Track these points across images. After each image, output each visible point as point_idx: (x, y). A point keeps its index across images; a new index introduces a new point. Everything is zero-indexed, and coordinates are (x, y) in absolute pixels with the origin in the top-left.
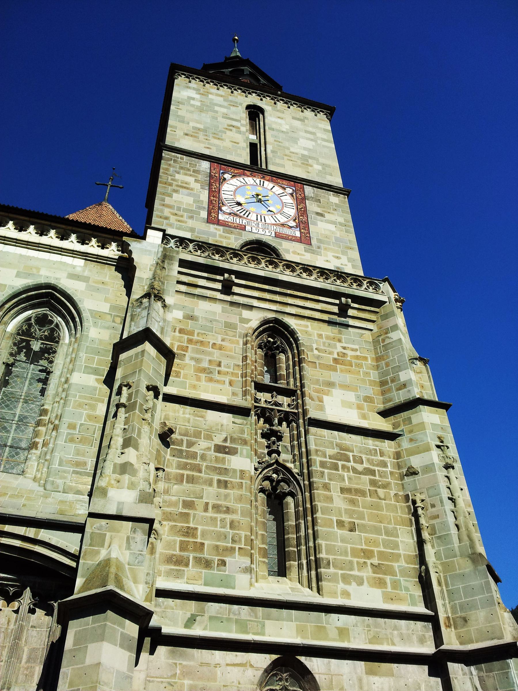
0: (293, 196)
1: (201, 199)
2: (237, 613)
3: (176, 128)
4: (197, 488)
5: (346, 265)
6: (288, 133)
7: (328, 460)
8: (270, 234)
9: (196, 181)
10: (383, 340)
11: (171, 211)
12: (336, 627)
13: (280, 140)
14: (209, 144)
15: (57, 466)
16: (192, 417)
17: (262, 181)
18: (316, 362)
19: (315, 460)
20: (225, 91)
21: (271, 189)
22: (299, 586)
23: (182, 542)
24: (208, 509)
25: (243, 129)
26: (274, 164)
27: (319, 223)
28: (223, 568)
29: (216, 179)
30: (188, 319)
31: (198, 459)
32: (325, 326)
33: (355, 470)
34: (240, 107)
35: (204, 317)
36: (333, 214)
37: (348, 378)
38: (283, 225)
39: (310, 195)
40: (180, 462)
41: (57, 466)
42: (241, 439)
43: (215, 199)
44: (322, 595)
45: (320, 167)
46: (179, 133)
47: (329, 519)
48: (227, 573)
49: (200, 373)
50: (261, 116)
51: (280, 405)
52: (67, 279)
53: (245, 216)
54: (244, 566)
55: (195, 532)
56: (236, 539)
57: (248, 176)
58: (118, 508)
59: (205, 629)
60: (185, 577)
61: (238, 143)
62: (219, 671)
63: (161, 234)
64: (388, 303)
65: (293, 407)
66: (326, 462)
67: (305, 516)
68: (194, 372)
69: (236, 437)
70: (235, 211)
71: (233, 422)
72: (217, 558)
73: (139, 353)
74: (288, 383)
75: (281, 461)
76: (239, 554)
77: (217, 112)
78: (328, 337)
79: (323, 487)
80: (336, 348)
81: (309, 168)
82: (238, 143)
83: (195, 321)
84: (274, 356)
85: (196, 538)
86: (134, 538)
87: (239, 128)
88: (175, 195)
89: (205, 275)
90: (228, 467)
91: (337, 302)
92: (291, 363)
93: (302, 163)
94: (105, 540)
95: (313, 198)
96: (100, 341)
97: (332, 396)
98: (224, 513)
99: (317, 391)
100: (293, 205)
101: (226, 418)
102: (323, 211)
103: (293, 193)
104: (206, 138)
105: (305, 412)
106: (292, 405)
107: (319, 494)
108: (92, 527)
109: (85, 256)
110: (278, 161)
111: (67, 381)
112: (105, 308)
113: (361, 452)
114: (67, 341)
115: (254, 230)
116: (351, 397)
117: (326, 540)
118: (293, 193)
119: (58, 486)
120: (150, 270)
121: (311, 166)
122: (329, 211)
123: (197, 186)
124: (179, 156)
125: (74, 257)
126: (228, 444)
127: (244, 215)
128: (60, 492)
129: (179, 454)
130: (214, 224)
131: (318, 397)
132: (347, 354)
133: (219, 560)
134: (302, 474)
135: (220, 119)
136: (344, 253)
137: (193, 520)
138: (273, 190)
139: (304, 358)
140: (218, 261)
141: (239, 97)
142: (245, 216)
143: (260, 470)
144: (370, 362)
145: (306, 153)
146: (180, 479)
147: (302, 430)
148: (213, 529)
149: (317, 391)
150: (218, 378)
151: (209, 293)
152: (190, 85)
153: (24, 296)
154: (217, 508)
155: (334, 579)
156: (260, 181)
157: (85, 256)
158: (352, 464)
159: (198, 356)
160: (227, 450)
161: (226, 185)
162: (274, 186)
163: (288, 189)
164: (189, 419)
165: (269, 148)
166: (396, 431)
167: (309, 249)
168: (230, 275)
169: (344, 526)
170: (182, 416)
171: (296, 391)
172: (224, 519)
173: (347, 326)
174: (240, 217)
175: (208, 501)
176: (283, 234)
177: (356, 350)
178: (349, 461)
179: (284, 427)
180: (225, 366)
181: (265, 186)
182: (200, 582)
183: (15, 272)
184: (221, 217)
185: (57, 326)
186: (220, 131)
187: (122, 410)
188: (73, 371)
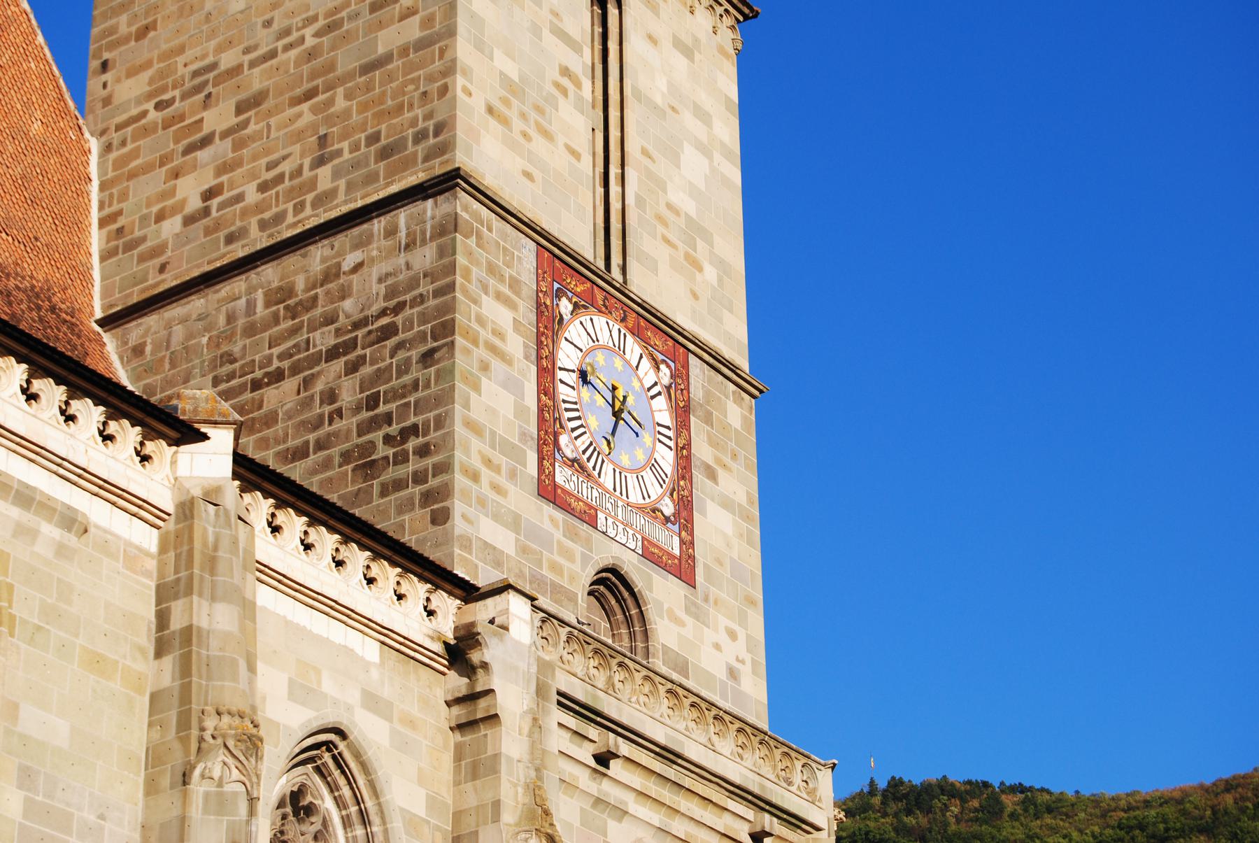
5: (743, 662)
64: (824, 834)
102: (718, 460)
109: (384, 633)
115: (612, 533)
145: (689, 206)
163: (663, 367)
184: (563, 476)
185: (325, 823)
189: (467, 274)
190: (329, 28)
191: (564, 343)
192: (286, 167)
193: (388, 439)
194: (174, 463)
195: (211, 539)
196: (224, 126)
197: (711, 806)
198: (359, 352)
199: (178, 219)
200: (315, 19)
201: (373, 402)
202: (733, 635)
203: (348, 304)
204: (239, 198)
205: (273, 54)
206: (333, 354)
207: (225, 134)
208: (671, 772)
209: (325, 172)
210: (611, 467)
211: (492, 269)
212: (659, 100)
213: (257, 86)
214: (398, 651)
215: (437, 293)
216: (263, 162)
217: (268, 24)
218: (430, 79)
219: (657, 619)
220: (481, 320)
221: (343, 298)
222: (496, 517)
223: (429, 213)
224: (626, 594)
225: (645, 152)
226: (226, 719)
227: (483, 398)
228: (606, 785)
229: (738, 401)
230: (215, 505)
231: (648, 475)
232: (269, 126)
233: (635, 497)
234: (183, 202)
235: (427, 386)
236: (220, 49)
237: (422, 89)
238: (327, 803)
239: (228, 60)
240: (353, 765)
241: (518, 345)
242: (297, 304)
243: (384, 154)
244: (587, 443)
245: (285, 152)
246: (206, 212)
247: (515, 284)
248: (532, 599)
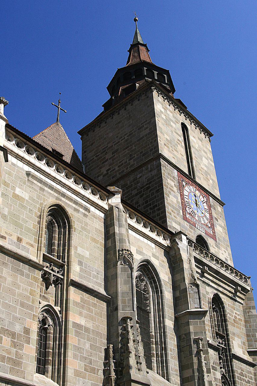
10: (248, 313)
14: (174, 154)
38: (207, 225)
70: (191, 211)
77: (172, 126)
114: (151, 294)
124: (166, 163)
134: (230, 381)
145: (205, 169)
163: (204, 198)
166: (253, 362)
173: (236, 301)
184: (188, 216)
185: (146, 283)
189: (164, 174)
190: (130, 135)
191: (185, 190)
192: (123, 162)
193: (150, 209)
194: (108, 201)
195: (117, 215)
196: (110, 157)
198: (142, 193)
199: (102, 176)
200: (127, 134)
201: (147, 202)
202: (225, 252)
203: (139, 184)
204: (115, 169)
205: (119, 142)
206: (136, 195)
207: (110, 159)
209: (132, 160)
210: (197, 216)
211: (169, 174)
212: (197, 148)
213: (116, 148)
215: (158, 178)
216: (119, 162)
217: (117, 137)
218: (152, 139)
219: (210, 247)
220: (168, 183)
221: (138, 184)
222: (175, 222)
223: (155, 164)
225: (195, 157)
226: (124, 252)
228: (204, 279)
229: (220, 207)
230: (118, 208)
231: (204, 218)
232: (119, 155)
233: (203, 222)
234: (103, 173)
235: (158, 196)
236: (108, 144)
237: (151, 141)
239: (109, 145)
241: (175, 189)
242: (128, 187)
243: (144, 155)
244: (192, 210)
245: (124, 159)
246: (108, 173)
247: (174, 177)
248: (186, 236)
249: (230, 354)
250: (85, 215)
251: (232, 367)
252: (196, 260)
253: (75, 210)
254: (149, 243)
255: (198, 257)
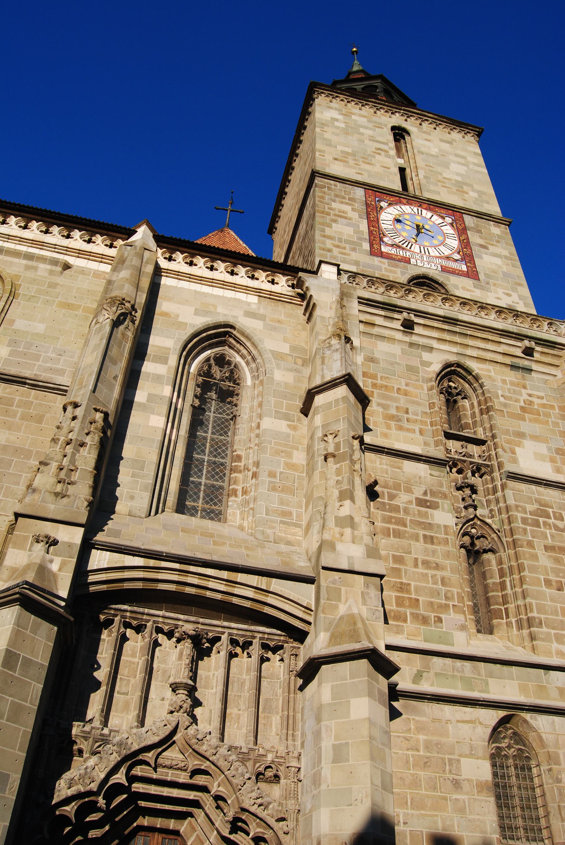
0: (453, 226)
1: (361, 229)
2: (460, 670)
3: (324, 152)
4: (405, 542)
5: (518, 303)
6: (437, 157)
7: (529, 516)
8: (436, 268)
9: (353, 210)
11: (333, 242)
12: (556, 687)
13: (431, 165)
14: (360, 169)
15: (264, 516)
16: (389, 469)
17: (420, 209)
18: (503, 411)
19: (516, 516)
20: (368, 111)
21: (430, 218)
22: (510, 644)
23: (397, 598)
24: (417, 565)
25: (393, 152)
26: (428, 191)
27: (484, 256)
28: (439, 624)
29: (373, 207)
30: (369, 361)
31: (402, 513)
32: (508, 369)
33: (557, 528)
34: (385, 129)
35: (385, 360)
36: (496, 246)
37: (537, 429)
38: (448, 258)
39: (470, 226)
40: (384, 515)
41: (264, 516)
42: (440, 493)
43: (375, 229)
44: (538, 655)
45: (475, 195)
46: (329, 158)
47: (536, 577)
48: (444, 630)
49: (389, 420)
50: (407, 137)
51: (471, 456)
52: (245, 318)
53: (408, 248)
54: (459, 623)
55: (408, 587)
56: (449, 595)
57: (405, 204)
58: (349, 562)
59: (432, 685)
60: (406, 633)
61: (389, 168)
62: (450, 727)
63: (335, 269)
65: (484, 458)
66: (528, 518)
67: (511, 574)
68: (383, 419)
69: (436, 490)
70: (397, 242)
71: (431, 475)
72: (433, 615)
73: (339, 399)
74: (475, 433)
75: (478, 515)
76: (454, 611)
77: (362, 134)
78: (512, 383)
79: (527, 544)
80: (521, 395)
81: (465, 195)
82: (389, 168)
83: (377, 363)
84: (455, 402)
85: (411, 594)
86: (368, 593)
87: (386, 151)
88: (334, 225)
89: (382, 313)
90: (432, 522)
91: (519, 344)
92: (477, 410)
93: (457, 190)
94: (341, 595)
95: (474, 228)
96: (286, 384)
97: (524, 447)
98: (434, 569)
99: (508, 442)
100: (455, 236)
101: (422, 469)
103: (453, 223)
104: (356, 162)
105: (500, 465)
106: (484, 456)
107: (524, 552)
108: (326, 581)
109: (258, 291)
110: (432, 187)
111: (258, 427)
112: (285, 349)
113: (560, 508)
116: (542, 448)
117: (536, 599)
118: (453, 223)
119: (268, 536)
120: (331, 308)
121: (467, 193)
122: (492, 243)
123: (355, 215)
125: (248, 294)
126: (428, 498)
127: (407, 246)
128: (271, 542)
129: (383, 507)
130: (378, 256)
131: (510, 449)
132: (533, 402)
133: (435, 617)
135: (367, 142)
136: (515, 290)
137: (405, 575)
138: (432, 219)
139: (492, 406)
140: (394, 297)
141: (383, 117)
142: (408, 248)
143: (460, 526)
144: (557, 411)
145: (459, 179)
146: (387, 533)
147: (499, 483)
148: (424, 585)
149: (508, 442)
150: (408, 427)
151: (387, 333)
152: (332, 105)
153: (204, 335)
154: (426, 563)
155: (547, 639)
156: (418, 210)
157: (258, 291)
158: (552, 521)
159: (384, 402)
160: (429, 504)
161: (383, 213)
162: (432, 216)
163: (447, 218)
164: (387, 470)
165: (421, 173)
167: (478, 285)
168: (409, 313)
169: (551, 585)
170: (379, 466)
171: (486, 441)
172: (435, 575)
174: (403, 249)
175: (416, 557)
176: (450, 268)
177: (542, 398)
178: (550, 518)
179: (476, 480)
180: (413, 414)
181: (424, 215)
182: (420, 638)
183: (193, 309)
184: (384, 249)
185: (236, 366)
186: (369, 155)
187: (330, 460)
188: (260, 416)
197: (490, 342)
208: (457, 329)
210: (417, 247)
214: (270, 298)
224: (437, 286)
227: (333, 229)
238: (238, 359)
240: (242, 339)
247: (352, 200)
249: (500, 474)
250: (51, 272)
251: (505, 502)
252: (364, 301)
253: (27, 268)
254: (241, 296)
255: (366, 294)
